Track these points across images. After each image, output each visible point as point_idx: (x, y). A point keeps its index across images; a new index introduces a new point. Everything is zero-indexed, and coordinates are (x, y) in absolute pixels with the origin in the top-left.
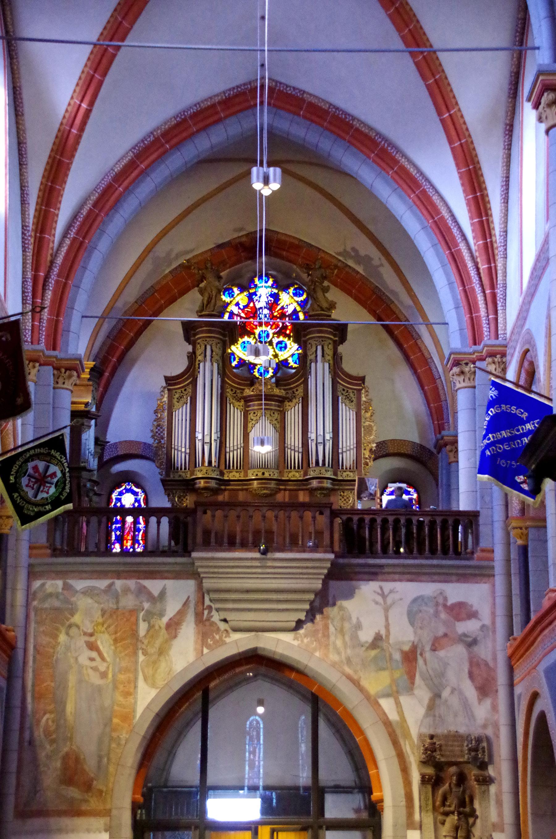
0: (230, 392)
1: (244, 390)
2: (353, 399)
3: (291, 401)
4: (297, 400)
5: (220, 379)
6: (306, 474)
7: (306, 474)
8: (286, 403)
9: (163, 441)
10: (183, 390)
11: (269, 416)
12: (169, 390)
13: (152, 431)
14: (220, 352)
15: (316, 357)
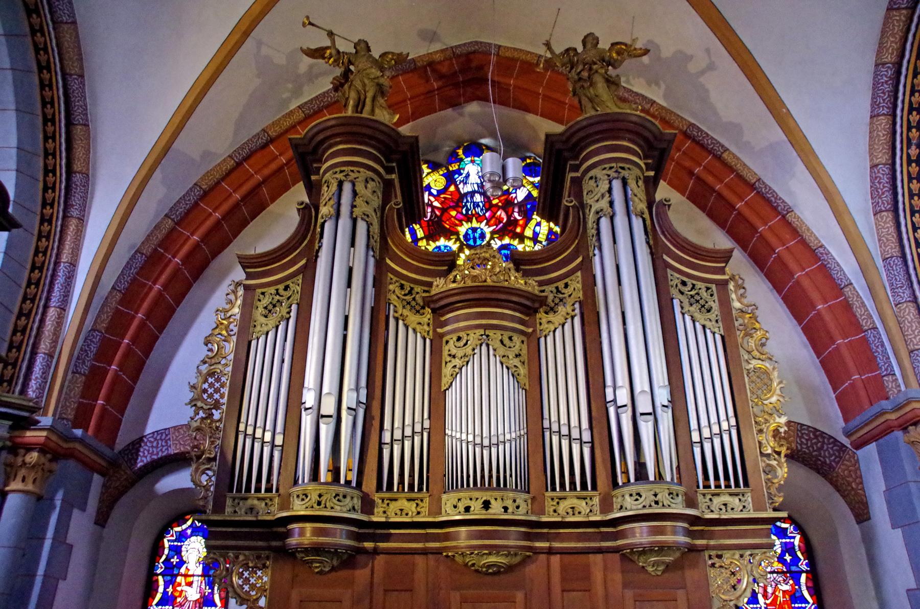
0: (398, 291)
1: (430, 285)
2: (711, 303)
3: (552, 310)
4: (569, 309)
5: (372, 261)
6: (606, 505)
7: (606, 505)
8: (541, 315)
9: (217, 415)
10: (281, 287)
11: (498, 344)
12: (247, 288)
13: (193, 387)
14: (376, 202)
15: (611, 204)
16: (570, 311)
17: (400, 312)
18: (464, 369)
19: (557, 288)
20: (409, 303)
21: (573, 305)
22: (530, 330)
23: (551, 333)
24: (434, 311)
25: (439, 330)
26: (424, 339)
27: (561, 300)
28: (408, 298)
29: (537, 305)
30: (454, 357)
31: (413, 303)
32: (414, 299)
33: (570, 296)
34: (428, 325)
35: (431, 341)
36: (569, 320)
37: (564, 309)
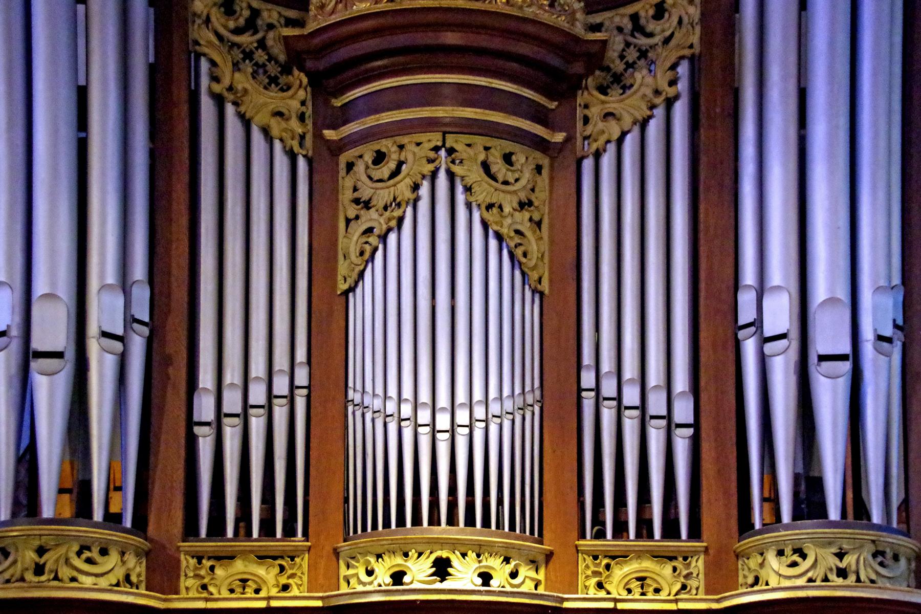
3: (618, 81)
16: (663, 84)
17: (226, 82)
19: (635, 18)
20: (248, 55)
22: (559, 137)
23: (612, 148)
25: (329, 134)
26: (292, 157)
27: (643, 54)
28: (245, 39)
29: (578, 68)
32: (262, 44)
34: (302, 118)
35: (310, 161)
36: (659, 112)
37: (649, 80)
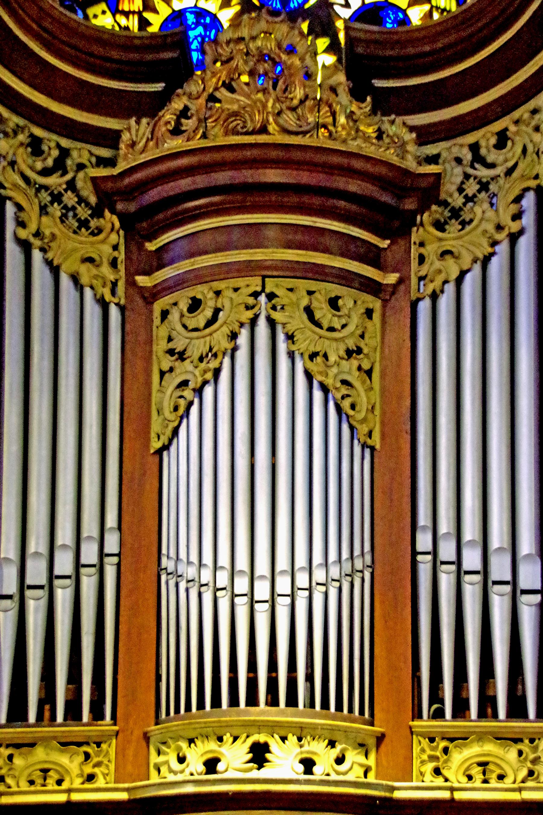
8: (424, 232)
16: (506, 219)
17: (33, 227)
18: (208, 391)
20: (57, 198)
21: (518, 200)
22: (392, 278)
23: (450, 288)
24: (128, 222)
25: (142, 280)
27: (484, 186)
29: (410, 205)
30: (182, 356)
31: (70, 199)
32: (71, 185)
33: (509, 172)
34: (114, 263)
35: (122, 309)
36: (503, 248)
37: (490, 214)
